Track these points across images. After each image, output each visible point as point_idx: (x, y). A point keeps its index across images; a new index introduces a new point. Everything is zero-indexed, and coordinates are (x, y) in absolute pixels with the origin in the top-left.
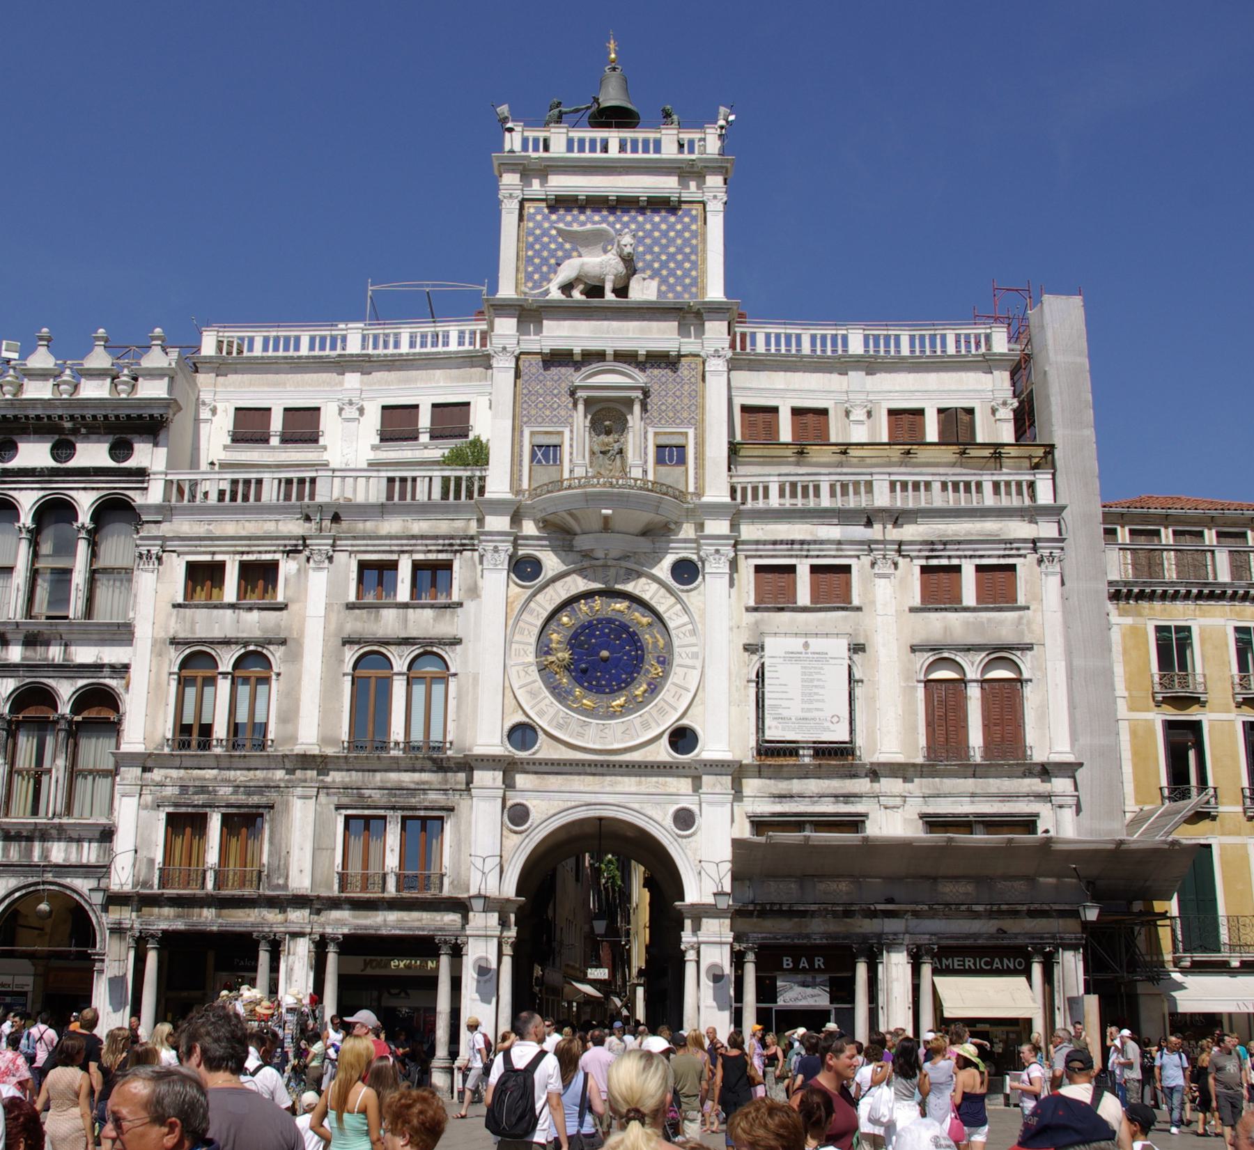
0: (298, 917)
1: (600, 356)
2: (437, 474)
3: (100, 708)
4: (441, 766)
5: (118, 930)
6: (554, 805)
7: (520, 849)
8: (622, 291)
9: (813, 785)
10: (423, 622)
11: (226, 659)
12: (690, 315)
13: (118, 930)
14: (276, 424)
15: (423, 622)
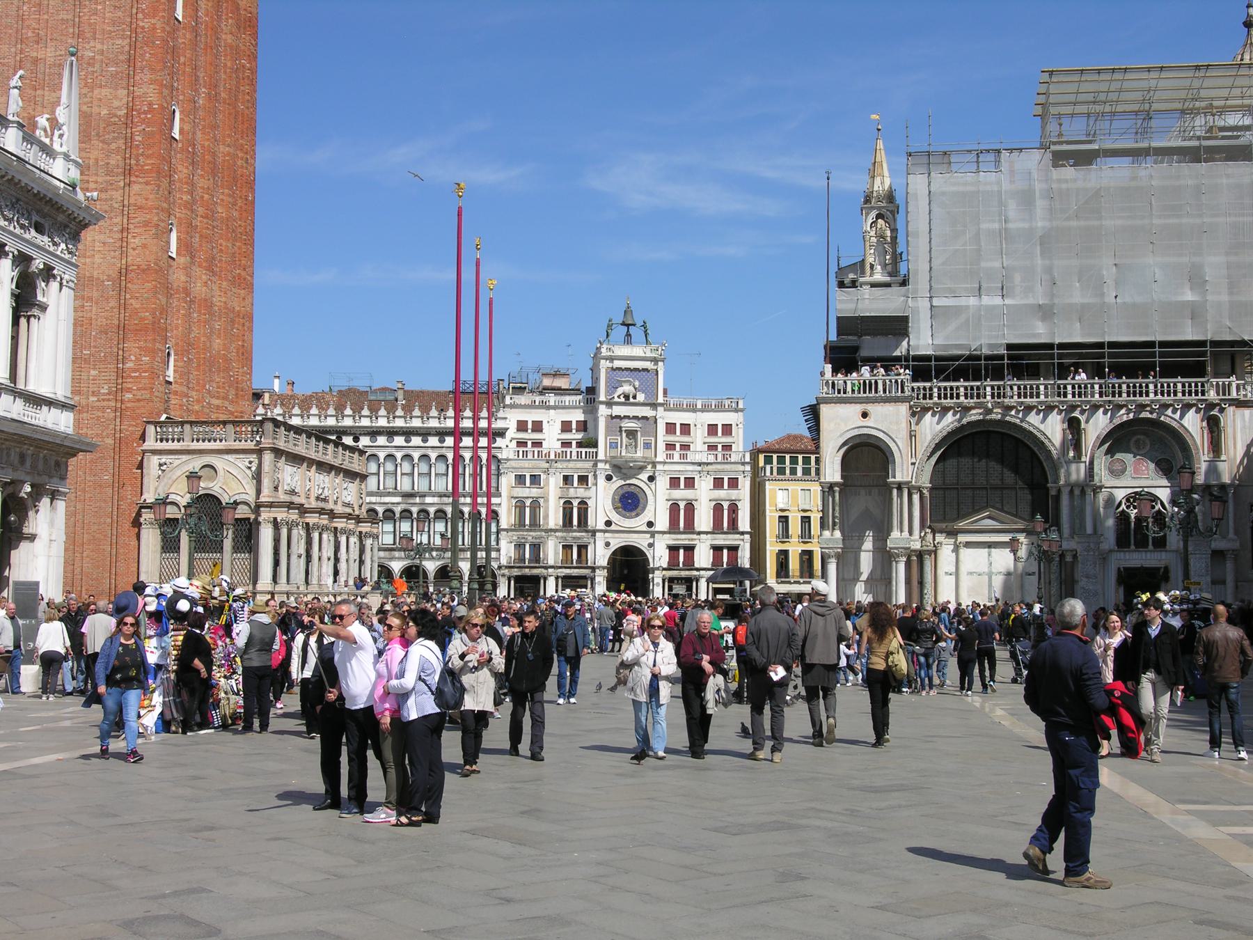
0: (550, 570)
1: (628, 417)
2: (584, 450)
3: (494, 515)
4: (587, 531)
5: (503, 575)
6: (617, 542)
7: (609, 553)
8: (634, 397)
9: (683, 536)
10: (581, 492)
11: (528, 503)
12: (654, 406)
13: (503, 575)
14: (530, 426)
15: (581, 492)
